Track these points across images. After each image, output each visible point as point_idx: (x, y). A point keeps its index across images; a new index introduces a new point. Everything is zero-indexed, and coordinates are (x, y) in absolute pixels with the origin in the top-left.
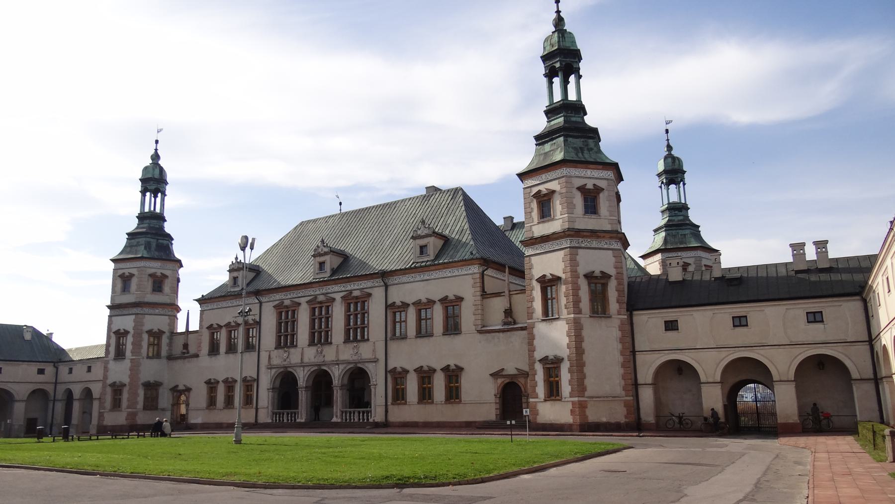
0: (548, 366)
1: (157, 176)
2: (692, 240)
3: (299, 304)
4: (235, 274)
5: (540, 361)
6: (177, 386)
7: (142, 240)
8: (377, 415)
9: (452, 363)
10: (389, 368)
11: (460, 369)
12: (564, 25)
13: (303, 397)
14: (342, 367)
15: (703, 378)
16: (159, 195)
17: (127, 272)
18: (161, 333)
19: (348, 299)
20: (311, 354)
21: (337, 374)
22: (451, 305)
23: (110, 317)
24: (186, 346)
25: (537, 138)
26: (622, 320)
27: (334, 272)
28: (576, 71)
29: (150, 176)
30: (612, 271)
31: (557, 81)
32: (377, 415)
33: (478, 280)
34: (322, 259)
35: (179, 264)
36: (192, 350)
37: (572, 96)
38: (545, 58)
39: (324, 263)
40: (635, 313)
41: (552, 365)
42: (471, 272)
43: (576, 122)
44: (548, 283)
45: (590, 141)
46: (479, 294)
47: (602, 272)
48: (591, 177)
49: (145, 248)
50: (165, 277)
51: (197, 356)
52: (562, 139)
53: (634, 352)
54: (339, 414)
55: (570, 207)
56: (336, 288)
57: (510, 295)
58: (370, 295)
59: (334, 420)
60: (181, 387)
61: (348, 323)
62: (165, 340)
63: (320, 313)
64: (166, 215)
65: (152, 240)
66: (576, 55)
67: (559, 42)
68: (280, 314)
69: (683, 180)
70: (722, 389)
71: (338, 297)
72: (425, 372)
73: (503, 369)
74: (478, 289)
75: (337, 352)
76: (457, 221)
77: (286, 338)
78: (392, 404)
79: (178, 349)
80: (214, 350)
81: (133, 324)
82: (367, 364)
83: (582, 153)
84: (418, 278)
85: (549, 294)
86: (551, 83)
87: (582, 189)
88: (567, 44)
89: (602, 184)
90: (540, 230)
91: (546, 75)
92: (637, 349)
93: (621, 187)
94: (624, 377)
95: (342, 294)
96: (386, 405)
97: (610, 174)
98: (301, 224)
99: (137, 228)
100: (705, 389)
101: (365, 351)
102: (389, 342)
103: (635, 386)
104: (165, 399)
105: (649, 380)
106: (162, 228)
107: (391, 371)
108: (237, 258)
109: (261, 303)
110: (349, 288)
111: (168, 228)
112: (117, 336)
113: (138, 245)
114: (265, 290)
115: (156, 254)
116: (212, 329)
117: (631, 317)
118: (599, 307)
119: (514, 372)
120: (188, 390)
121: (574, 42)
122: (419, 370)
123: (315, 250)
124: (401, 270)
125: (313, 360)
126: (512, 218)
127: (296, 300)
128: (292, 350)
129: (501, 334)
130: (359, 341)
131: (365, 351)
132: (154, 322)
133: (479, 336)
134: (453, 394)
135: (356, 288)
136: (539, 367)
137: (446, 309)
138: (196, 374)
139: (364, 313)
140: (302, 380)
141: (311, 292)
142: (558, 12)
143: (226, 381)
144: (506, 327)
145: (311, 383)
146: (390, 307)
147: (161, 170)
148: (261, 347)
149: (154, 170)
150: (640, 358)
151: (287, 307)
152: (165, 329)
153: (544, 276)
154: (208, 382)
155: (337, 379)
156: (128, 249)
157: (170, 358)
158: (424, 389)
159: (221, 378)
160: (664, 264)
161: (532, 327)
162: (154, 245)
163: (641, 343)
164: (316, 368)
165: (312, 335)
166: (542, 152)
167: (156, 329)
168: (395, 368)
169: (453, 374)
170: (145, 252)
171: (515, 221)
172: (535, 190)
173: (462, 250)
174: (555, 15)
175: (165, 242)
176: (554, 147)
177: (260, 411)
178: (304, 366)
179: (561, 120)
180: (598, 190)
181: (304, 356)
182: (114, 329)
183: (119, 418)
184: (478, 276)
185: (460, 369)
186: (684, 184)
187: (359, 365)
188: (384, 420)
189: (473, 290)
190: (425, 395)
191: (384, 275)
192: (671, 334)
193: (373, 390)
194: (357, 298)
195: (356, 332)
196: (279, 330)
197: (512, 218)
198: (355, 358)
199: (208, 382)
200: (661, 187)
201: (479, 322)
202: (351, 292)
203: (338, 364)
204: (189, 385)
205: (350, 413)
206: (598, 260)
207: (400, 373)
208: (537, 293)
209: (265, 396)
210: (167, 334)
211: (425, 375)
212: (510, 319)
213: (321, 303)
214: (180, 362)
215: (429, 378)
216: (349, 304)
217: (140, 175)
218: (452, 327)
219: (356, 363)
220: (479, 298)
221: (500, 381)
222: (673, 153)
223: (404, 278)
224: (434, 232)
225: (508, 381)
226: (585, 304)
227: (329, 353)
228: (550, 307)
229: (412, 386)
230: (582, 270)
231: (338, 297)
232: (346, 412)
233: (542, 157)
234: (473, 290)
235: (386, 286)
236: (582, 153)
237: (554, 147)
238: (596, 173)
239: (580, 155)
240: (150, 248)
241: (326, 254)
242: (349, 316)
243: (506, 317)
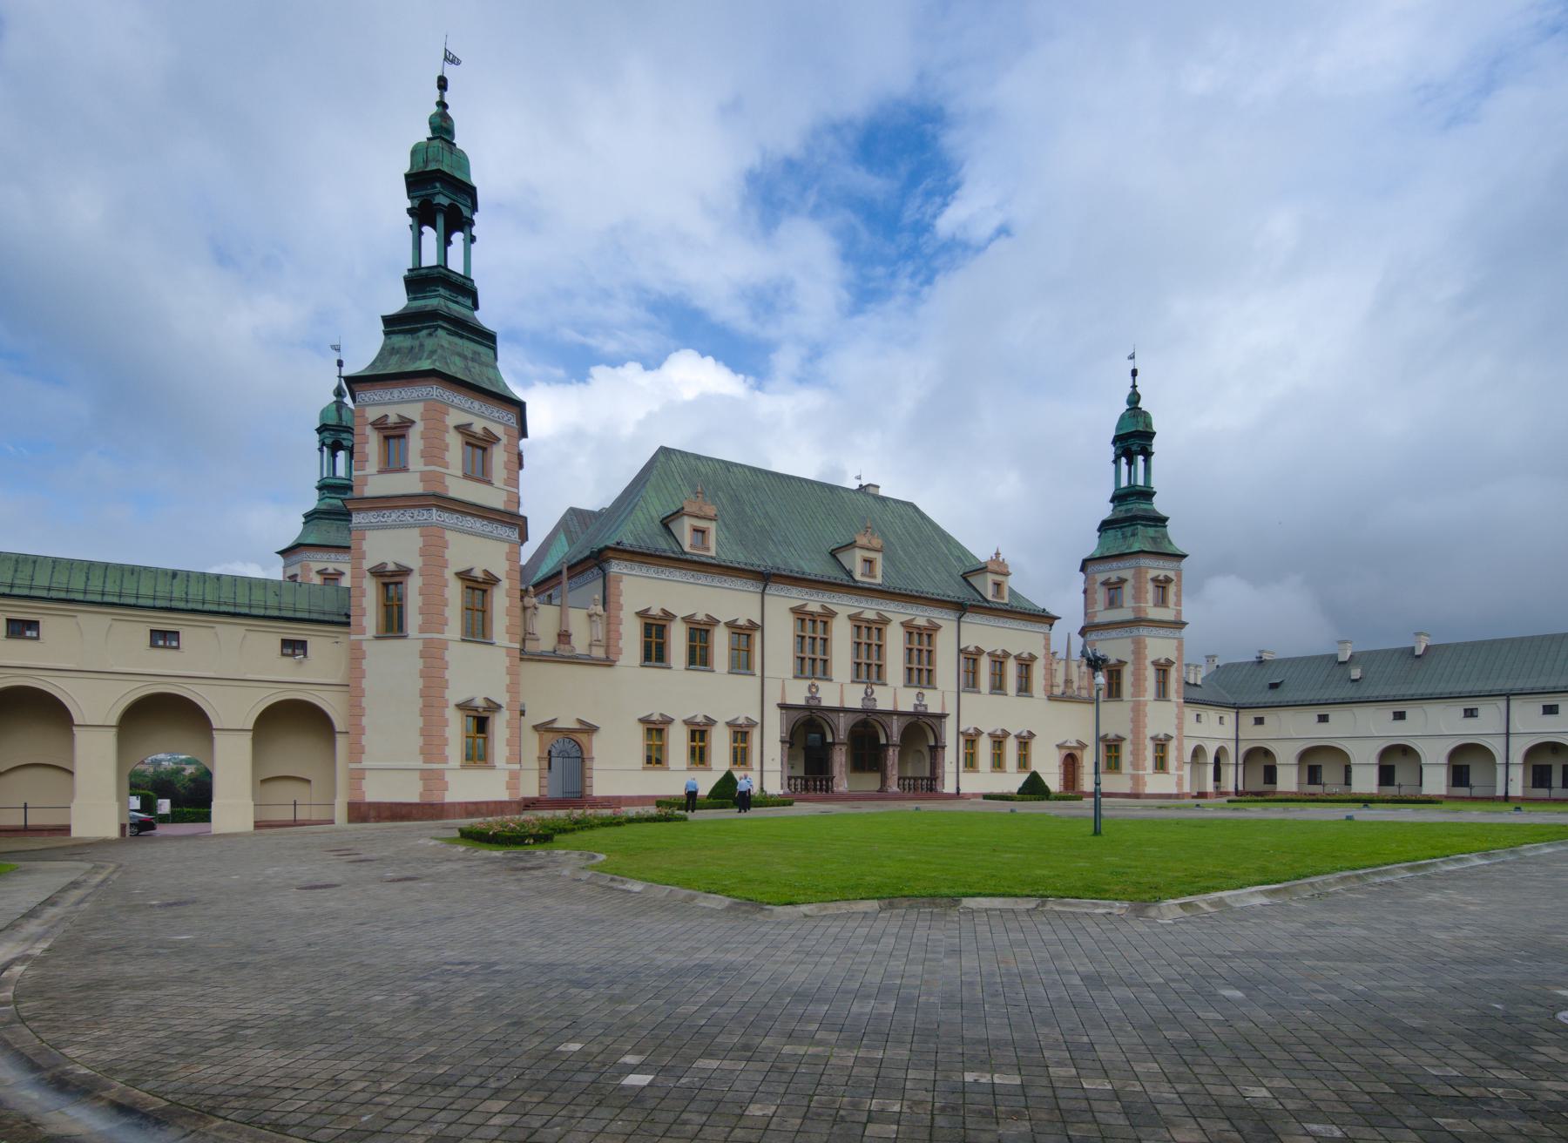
8: (949, 788)
32: (949, 788)
51: (608, 662)
77: (812, 662)
131: (933, 703)
142: (1134, 386)
195: (920, 673)
208: (1151, 674)
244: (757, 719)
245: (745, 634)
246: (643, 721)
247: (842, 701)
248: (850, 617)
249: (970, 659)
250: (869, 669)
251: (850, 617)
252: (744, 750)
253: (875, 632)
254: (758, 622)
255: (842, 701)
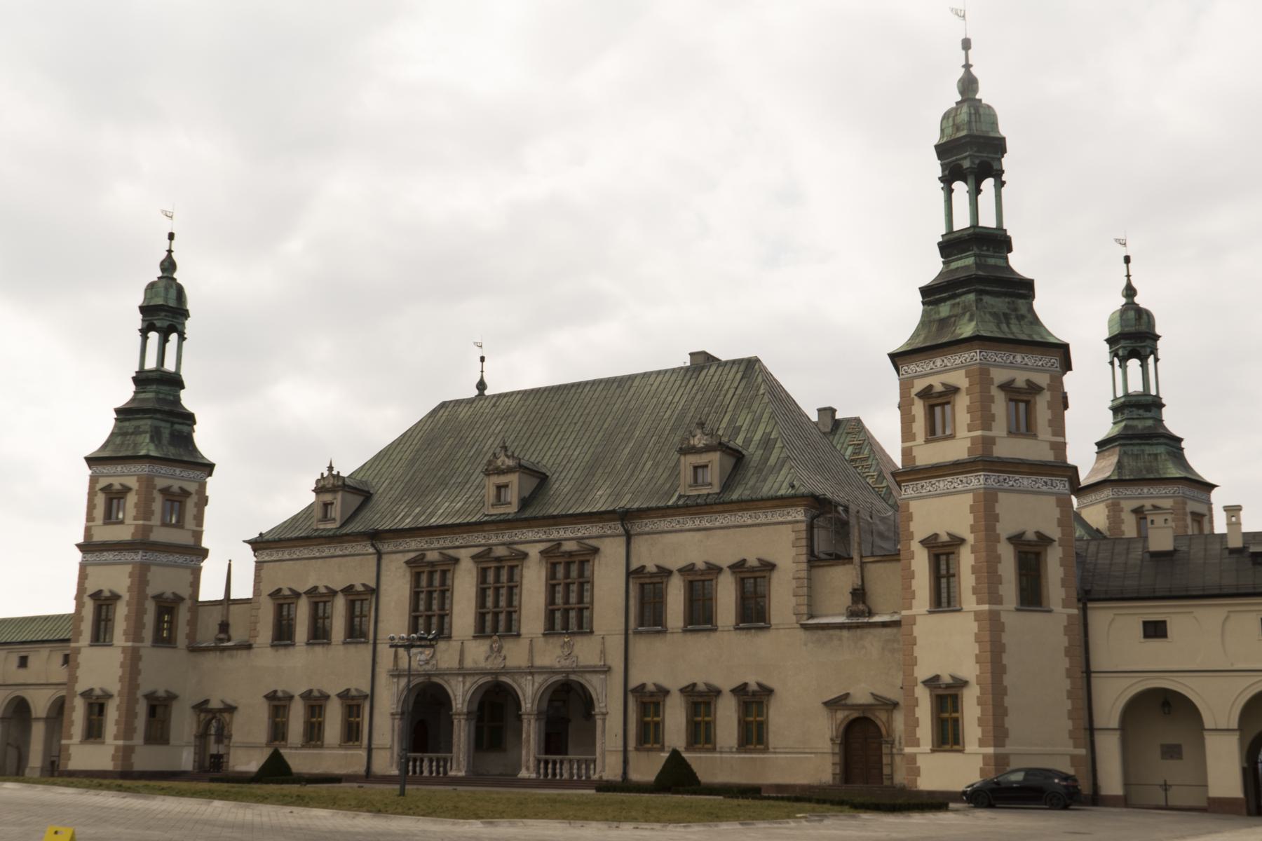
0: (940, 692)
1: (172, 303)
2: (1170, 465)
3: (456, 561)
4: (328, 497)
5: (925, 683)
6: (206, 702)
7: (146, 424)
8: (609, 768)
9: (752, 680)
10: (634, 683)
11: (766, 692)
12: (976, 91)
13: (462, 733)
14: (539, 679)
15: (1208, 723)
16: (174, 337)
17: (116, 483)
18: (178, 599)
19: (552, 556)
20: (478, 654)
21: (529, 692)
22: (753, 579)
23: (83, 567)
24: (224, 627)
25: (926, 292)
26: (1069, 616)
27: (525, 503)
28: (998, 174)
29: (160, 301)
30: (1054, 532)
31: (960, 188)
33: (804, 535)
34: (502, 480)
35: (209, 468)
36: (238, 634)
37: (987, 220)
38: (942, 150)
39: (506, 486)
40: (1089, 605)
41: (946, 697)
42: (790, 518)
43: (996, 267)
44: (942, 552)
45: (1021, 302)
46: (804, 558)
47: (1038, 534)
48: (1021, 369)
49: (152, 440)
50: (185, 493)
51: (248, 647)
52: (972, 297)
53: (1088, 673)
54: (532, 764)
55: (984, 418)
56: (530, 535)
57: (862, 564)
58: (595, 551)
59: (524, 774)
60: (215, 704)
61: (551, 600)
62: (183, 615)
63: (498, 579)
64: (185, 375)
65: (163, 424)
66: (999, 146)
67: (970, 122)
68: (416, 577)
69: (1154, 351)
70: (1241, 739)
71: (534, 551)
72: (701, 694)
73: (847, 695)
74: (804, 550)
75: (531, 651)
76: (756, 422)
77: (429, 620)
78: (637, 749)
79: (208, 631)
80: (283, 635)
81: (128, 582)
82: (588, 676)
83: (1008, 324)
84: (689, 525)
85: (943, 567)
86: (949, 192)
87: (1007, 387)
88: (984, 128)
89: (1042, 379)
90: (927, 455)
91: (941, 179)
92: (1093, 668)
93: (1068, 379)
94: (1071, 715)
95: (542, 547)
96: (625, 751)
97: (1054, 361)
98: (444, 405)
99: (133, 400)
100: (1211, 741)
101: (585, 652)
102: (631, 637)
103: (1088, 730)
104: (183, 724)
105: (1115, 723)
106: (177, 401)
107: (635, 691)
108: (331, 468)
109: (379, 555)
110: (555, 535)
111: (188, 399)
112: (100, 605)
113: (137, 432)
114: (390, 531)
115: (172, 452)
116: (283, 602)
117: (1084, 611)
118: (1031, 596)
119: (870, 700)
120: (231, 709)
121: (994, 124)
122: (689, 691)
123: (490, 463)
124: (658, 508)
125: (482, 664)
126: (833, 411)
127: (451, 552)
128: (442, 645)
129: (845, 633)
130: (574, 634)
131: (585, 652)
132: (164, 580)
133: (802, 634)
134: (753, 735)
135: (569, 538)
136: (924, 697)
137: (741, 583)
138: (245, 682)
139: (585, 583)
140: (460, 700)
141: (480, 539)
143: (307, 696)
144: (855, 620)
145: (475, 707)
146: (632, 574)
147: (180, 291)
148: (380, 636)
149: (167, 289)
150: (1097, 682)
151: (432, 564)
152: (185, 592)
153: (936, 536)
154: (271, 697)
155: (529, 701)
156: (118, 440)
157: (194, 649)
158: (697, 724)
159: (298, 689)
160: (1115, 509)
161: (912, 620)
162: (166, 434)
163: (1100, 660)
164: (488, 679)
165: (481, 618)
166: (937, 317)
167: (168, 594)
168: (643, 686)
169: (754, 701)
170: (152, 447)
171: (838, 416)
172: (920, 385)
173: (771, 479)
174: (961, 72)
175: (185, 428)
176: (958, 310)
177: (375, 753)
178: (464, 675)
179: (970, 261)
180: (1034, 388)
181: (464, 656)
182: (91, 588)
183: (100, 757)
184: (803, 526)
185: (766, 692)
186: (1156, 360)
187: (573, 677)
188: (619, 779)
189: (793, 552)
190: (700, 733)
191: (625, 517)
192: (1155, 644)
193: (599, 723)
194: (570, 554)
195: (569, 615)
196: (415, 607)
197: (833, 411)
198: (567, 663)
199: (271, 697)
200: (1112, 363)
201: (804, 609)
202: (559, 543)
203: (532, 674)
204: (230, 701)
205: (554, 763)
206: (1030, 511)
207: (652, 694)
208: (921, 562)
209: (385, 727)
210: (188, 603)
211: (701, 701)
212: (861, 607)
213: (498, 559)
214: (211, 655)
215: (708, 704)
216: (554, 565)
217: (139, 299)
218: (753, 613)
219: (568, 673)
220: (804, 566)
221: (841, 715)
222: (1137, 300)
223: (663, 524)
224: (720, 443)
225: (855, 715)
226: (1009, 589)
227: (515, 654)
228: (944, 591)
229: (675, 720)
230: (1006, 528)
231: (534, 551)
232: (546, 762)
233: (934, 328)
234: (793, 552)
235: (629, 537)
236: (1008, 324)
237: (958, 310)
238: (1030, 360)
239: (1004, 327)
240: (160, 440)
241: (509, 470)
242: (554, 586)
243: (855, 601)
244: (366, 689)
245: (362, 601)
246: (266, 697)
247: (461, 661)
248: (474, 557)
249: (647, 590)
250: (497, 620)
251: (474, 557)
252: (358, 724)
253: (437, 577)
254: (373, 585)
255: (461, 661)
